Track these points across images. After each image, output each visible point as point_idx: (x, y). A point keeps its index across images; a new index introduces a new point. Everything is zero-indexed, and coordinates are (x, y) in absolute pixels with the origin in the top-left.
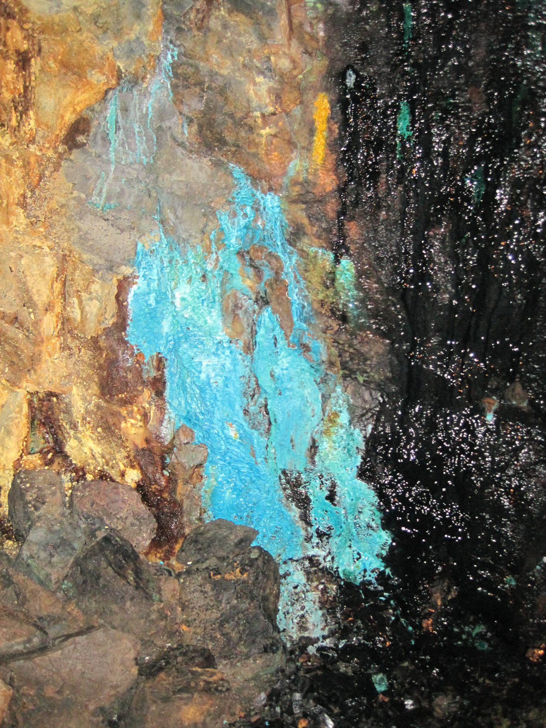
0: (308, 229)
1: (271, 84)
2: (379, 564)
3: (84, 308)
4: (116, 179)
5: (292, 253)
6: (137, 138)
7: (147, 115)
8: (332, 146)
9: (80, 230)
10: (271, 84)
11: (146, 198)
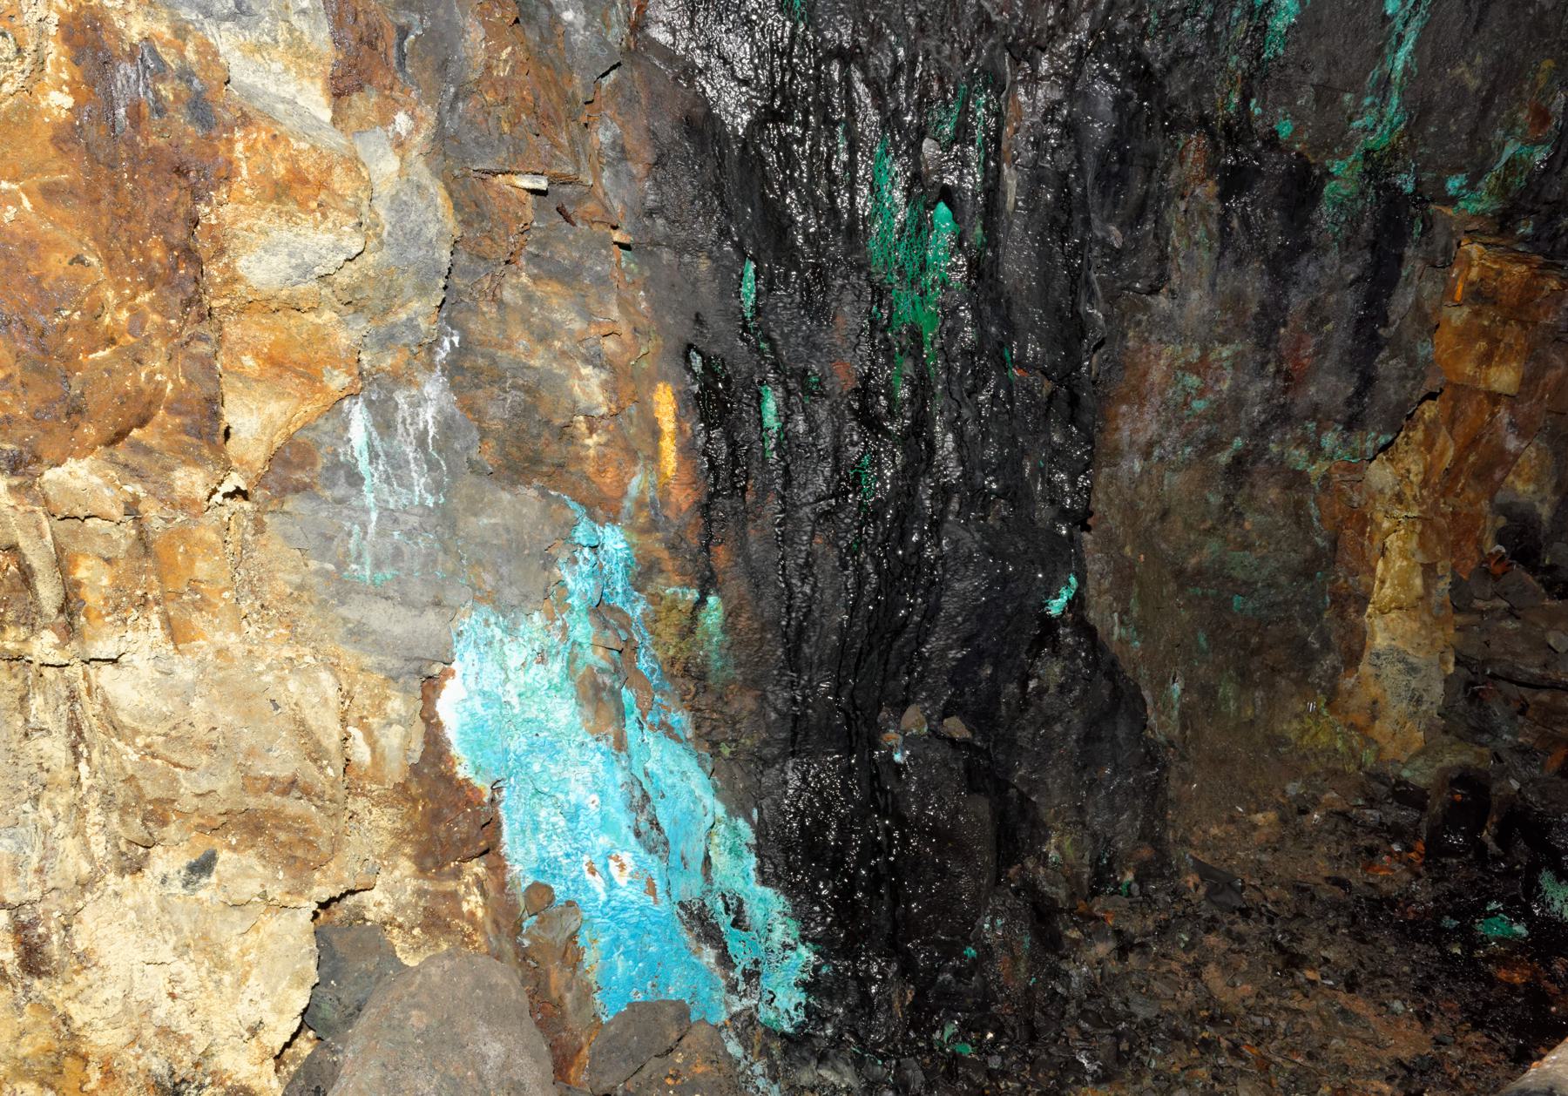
0: (669, 565)
1: (604, 376)
2: (800, 997)
3: (376, 742)
4: (381, 533)
5: (637, 600)
6: (412, 466)
7: (426, 431)
8: (686, 450)
9: (345, 620)
10: (604, 376)
11: (441, 557)
